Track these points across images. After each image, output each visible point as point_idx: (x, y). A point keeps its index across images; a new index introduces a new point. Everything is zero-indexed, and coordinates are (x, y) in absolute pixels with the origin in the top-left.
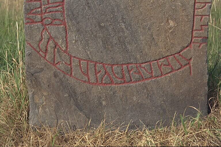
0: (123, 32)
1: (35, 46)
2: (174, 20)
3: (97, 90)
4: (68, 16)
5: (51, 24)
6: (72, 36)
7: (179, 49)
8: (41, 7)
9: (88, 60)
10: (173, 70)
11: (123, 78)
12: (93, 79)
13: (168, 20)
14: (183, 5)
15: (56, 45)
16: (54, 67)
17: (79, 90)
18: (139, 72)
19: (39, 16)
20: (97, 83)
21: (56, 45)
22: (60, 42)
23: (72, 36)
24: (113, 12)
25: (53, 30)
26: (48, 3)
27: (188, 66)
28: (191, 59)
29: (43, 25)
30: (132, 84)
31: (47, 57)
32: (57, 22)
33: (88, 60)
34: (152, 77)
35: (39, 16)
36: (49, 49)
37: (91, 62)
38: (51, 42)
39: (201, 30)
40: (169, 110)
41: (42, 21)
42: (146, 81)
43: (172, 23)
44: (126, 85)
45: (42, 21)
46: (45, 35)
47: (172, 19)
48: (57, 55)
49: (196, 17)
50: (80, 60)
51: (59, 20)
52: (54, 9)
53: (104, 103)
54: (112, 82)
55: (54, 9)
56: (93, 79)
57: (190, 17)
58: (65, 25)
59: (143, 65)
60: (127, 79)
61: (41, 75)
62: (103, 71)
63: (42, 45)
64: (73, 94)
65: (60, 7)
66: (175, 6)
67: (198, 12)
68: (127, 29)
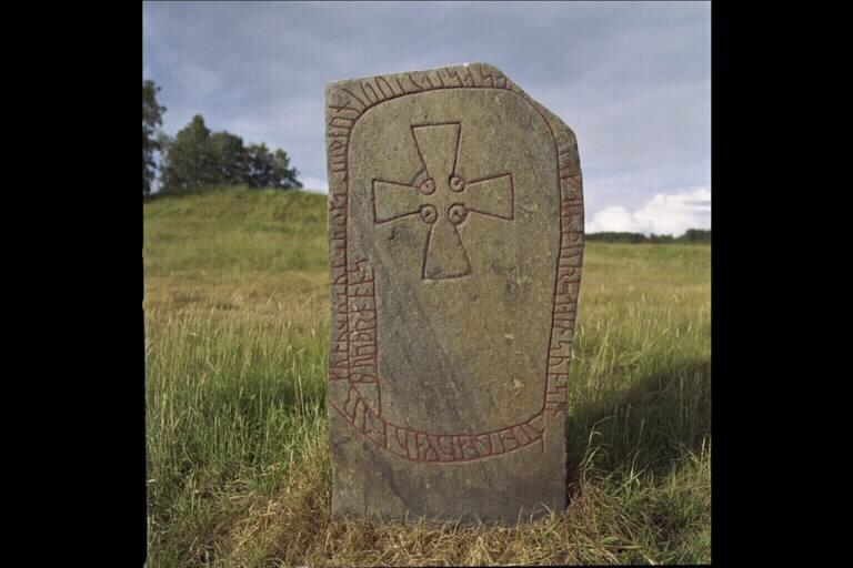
0: (454, 394)
1: (341, 408)
2: (520, 379)
3: (418, 469)
4: (382, 371)
5: (361, 380)
6: (387, 398)
7: (527, 417)
8: (348, 359)
9: (408, 429)
10: (519, 445)
11: (453, 453)
12: (413, 454)
13: (512, 379)
14: (533, 359)
15: (367, 408)
16: (363, 436)
17: (396, 468)
18: (474, 448)
19: (346, 371)
20: (418, 460)
21: (367, 408)
22: (371, 404)
23: (387, 398)
24: (440, 368)
25: (363, 389)
26: (358, 354)
27: (539, 441)
28: (543, 431)
29: (350, 382)
30: (464, 463)
31: (356, 424)
32: (368, 378)
33: (408, 429)
34: (491, 454)
35: (346, 371)
36: (358, 413)
37: (412, 431)
38: (360, 404)
39: (557, 393)
40: (511, 504)
41: (349, 376)
42: (484, 460)
43: (518, 384)
44: (457, 463)
45: (349, 376)
46: (354, 395)
47: (518, 378)
48: (368, 421)
49: (549, 377)
50: (397, 428)
51: (370, 376)
52: (362, 362)
53: (428, 486)
54: (438, 459)
55: (362, 362)
56: (413, 454)
57: (543, 376)
58: (378, 381)
59: (480, 438)
60: (458, 456)
61: (347, 446)
62: (426, 445)
63: (350, 407)
64: (388, 472)
65: (371, 361)
66: (523, 361)
67: (553, 369)
68: (458, 389)
